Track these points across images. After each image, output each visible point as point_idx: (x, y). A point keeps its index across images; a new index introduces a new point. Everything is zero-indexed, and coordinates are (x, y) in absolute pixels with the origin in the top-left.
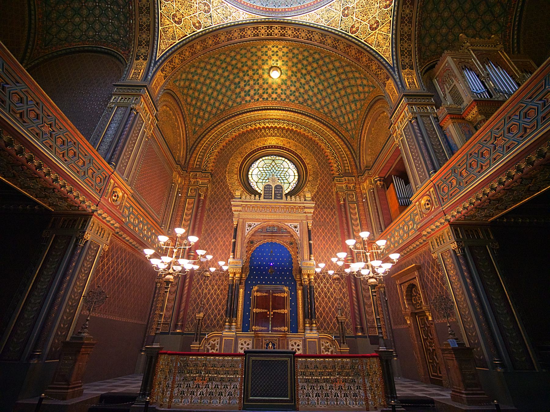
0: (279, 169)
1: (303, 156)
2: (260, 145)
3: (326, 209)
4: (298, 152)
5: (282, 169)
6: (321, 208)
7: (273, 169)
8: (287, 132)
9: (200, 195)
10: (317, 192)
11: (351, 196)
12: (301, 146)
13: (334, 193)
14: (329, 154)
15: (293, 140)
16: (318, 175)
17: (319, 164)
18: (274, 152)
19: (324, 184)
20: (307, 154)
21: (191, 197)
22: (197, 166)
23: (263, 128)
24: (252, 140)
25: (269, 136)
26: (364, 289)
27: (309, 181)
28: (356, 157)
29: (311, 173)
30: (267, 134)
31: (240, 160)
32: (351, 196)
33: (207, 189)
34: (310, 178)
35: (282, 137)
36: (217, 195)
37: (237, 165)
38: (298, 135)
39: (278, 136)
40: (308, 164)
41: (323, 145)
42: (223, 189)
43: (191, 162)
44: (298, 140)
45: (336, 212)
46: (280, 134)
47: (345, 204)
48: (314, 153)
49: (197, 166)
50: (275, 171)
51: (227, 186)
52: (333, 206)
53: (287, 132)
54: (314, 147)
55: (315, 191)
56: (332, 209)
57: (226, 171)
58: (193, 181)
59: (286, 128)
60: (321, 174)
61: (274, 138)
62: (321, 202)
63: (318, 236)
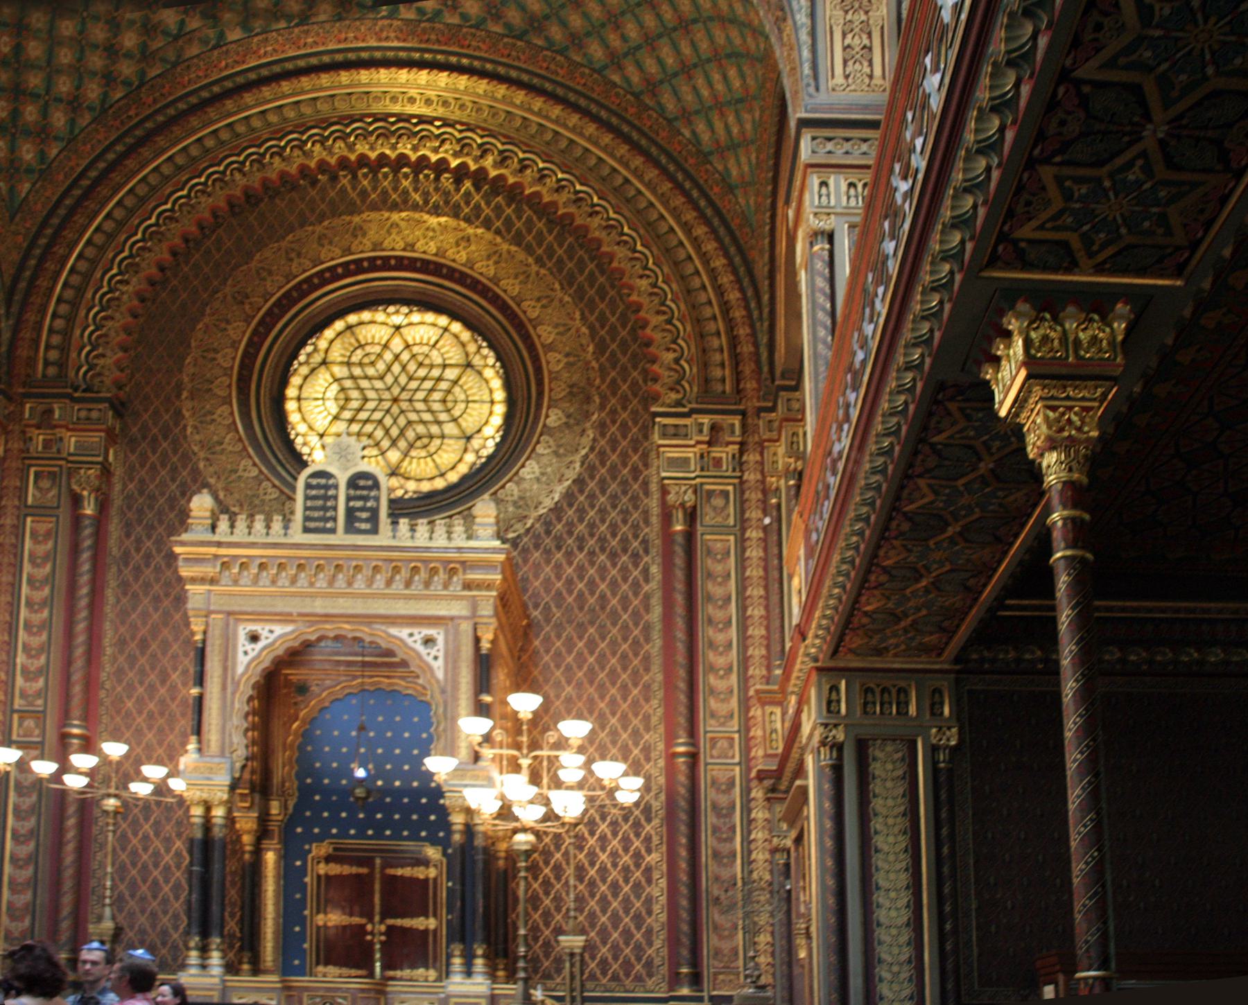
0: (422, 372)
1: (531, 310)
2: (334, 258)
3: (613, 556)
4: (510, 288)
5: (436, 373)
6: (592, 553)
7: (396, 368)
8: (458, 181)
9: (76, 500)
10: (580, 482)
11: (718, 502)
12: (521, 255)
13: (654, 487)
14: (645, 300)
15: (487, 224)
16: (588, 399)
17: (601, 348)
18: (396, 289)
19: (614, 443)
20: (546, 300)
21: (40, 511)
22: (52, 371)
23: (343, 163)
24: (291, 229)
25: (374, 207)
26: (716, 854)
27: (547, 430)
28: (761, 313)
29: (560, 390)
30: (364, 194)
31: (241, 333)
32: (718, 502)
33: (106, 471)
34: (554, 418)
35: (436, 211)
36: (152, 498)
37: (231, 359)
38: (511, 199)
39: (416, 207)
40: (549, 348)
41: (622, 252)
42: (174, 470)
43: (23, 352)
44: (508, 223)
45: (654, 569)
46: (426, 195)
47: (690, 536)
48: (580, 295)
49: (52, 371)
50: (403, 380)
51: (186, 458)
52: (645, 542)
53: (458, 181)
54: (581, 265)
55: (571, 475)
56: (636, 557)
57: (179, 388)
58: (39, 438)
59: (454, 163)
60: (604, 399)
61: (395, 217)
62: (592, 526)
63: (569, 668)
